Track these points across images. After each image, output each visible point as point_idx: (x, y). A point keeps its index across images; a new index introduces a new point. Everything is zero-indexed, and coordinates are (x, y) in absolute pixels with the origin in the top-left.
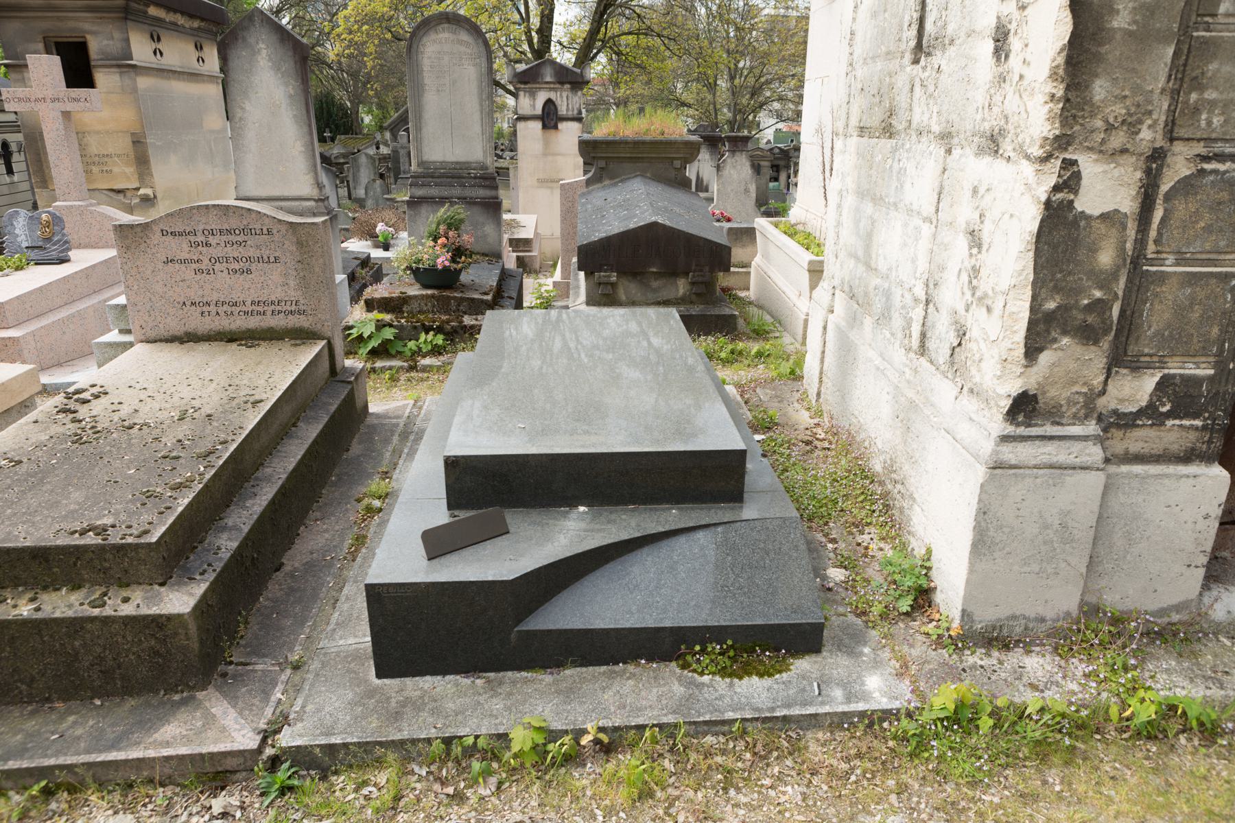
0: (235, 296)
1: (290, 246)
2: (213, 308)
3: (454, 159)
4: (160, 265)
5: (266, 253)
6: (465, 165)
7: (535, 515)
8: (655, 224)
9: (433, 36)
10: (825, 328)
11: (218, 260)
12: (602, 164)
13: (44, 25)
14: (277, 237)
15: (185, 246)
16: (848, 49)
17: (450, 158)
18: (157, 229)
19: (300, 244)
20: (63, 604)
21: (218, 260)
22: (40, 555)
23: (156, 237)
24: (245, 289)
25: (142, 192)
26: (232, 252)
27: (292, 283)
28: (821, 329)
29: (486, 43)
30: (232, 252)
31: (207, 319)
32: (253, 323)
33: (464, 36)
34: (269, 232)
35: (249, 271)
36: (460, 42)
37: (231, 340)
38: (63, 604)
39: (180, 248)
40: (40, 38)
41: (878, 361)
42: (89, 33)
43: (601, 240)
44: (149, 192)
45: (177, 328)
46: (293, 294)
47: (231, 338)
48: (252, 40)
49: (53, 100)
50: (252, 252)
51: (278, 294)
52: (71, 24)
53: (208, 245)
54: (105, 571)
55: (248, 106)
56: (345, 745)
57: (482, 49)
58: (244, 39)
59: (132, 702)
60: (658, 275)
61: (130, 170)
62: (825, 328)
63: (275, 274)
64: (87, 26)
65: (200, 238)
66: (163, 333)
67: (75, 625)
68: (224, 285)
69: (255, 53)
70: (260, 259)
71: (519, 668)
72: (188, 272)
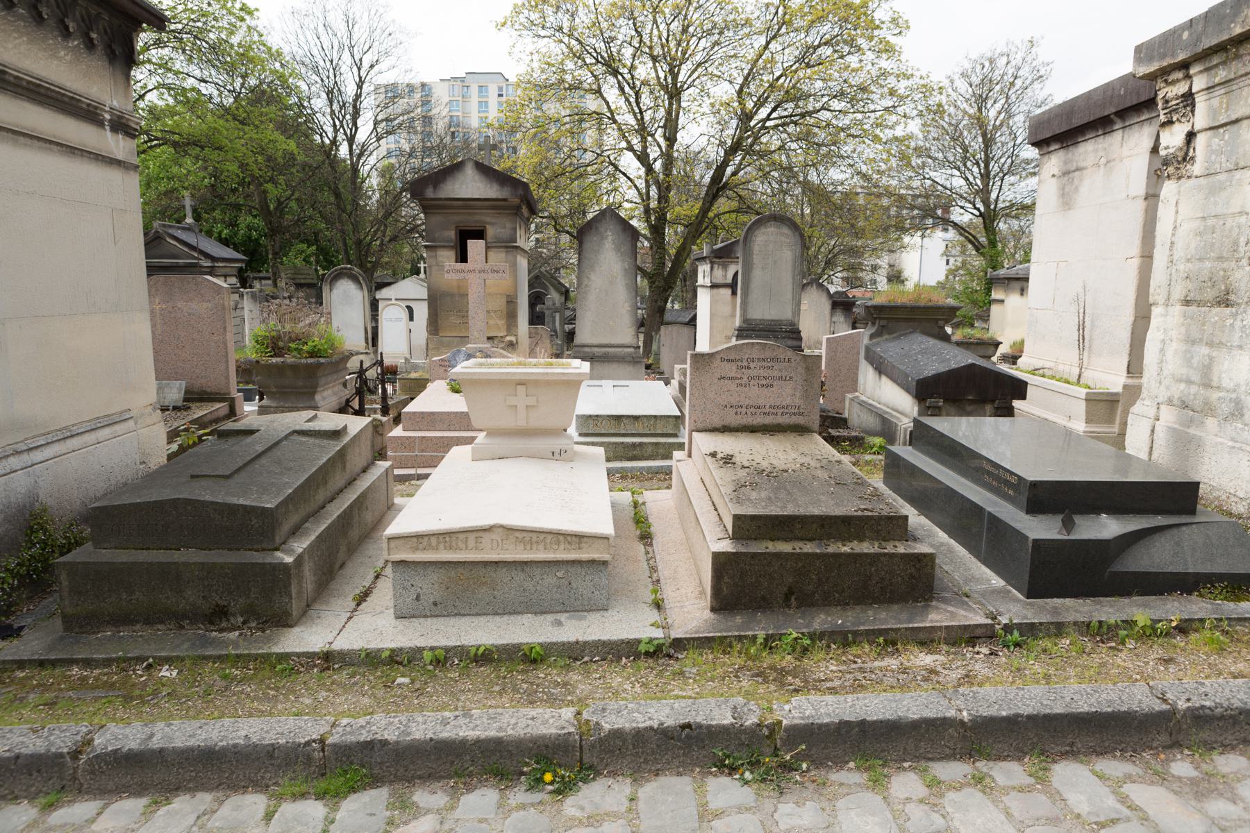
0: (761, 402)
1: (801, 370)
2: (744, 410)
3: (770, 318)
4: (716, 381)
5: (784, 374)
6: (778, 323)
7: (1086, 517)
8: (973, 365)
9: (763, 230)
10: (1153, 431)
11: (753, 378)
12: (883, 323)
13: (457, 218)
14: (793, 364)
15: (734, 368)
16: (1168, 252)
17: (767, 317)
18: (718, 357)
19: (807, 369)
20: (866, 547)
21: (753, 378)
22: (846, 520)
23: (717, 363)
24: (766, 397)
25: (508, 338)
26: (762, 373)
27: (798, 394)
28: (1149, 432)
29: (802, 236)
30: (762, 373)
31: (739, 417)
32: (768, 420)
33: (786, 230)
34: (789, 360)
35: (772, 386)
36: (782, 234)
37: (752, 431)
38: (866, 547)
39: (730, 370)
40: (453, 227)
41: (1230, 444)
42: (490, 223)
43: (934, 376)
44: (513, 339)
45: (717, 422)
46: (798, 401)
47: (752, 430)
48: (602, 229)
49: (480, 272)
50: (776, 374)
51: (788, 401)
52: (477, 218)
53: (749, 368)
54: (878, 532)
55: (593, 277)
56: (1041, 624)
57: (798, 239)
58: (597, 228)
59: (896, 607)
60: (972, 402)
61: (502, 322)
62: (1153, 431)
63: (788, 388)
64: (488, 219)
65: (745, 363)
66: (708, 425)
67: (874, 558)
68: (756, 395)
69: (603, 238)
70: (780, 378)
71: (1106, 596)
72: (732, 385)
